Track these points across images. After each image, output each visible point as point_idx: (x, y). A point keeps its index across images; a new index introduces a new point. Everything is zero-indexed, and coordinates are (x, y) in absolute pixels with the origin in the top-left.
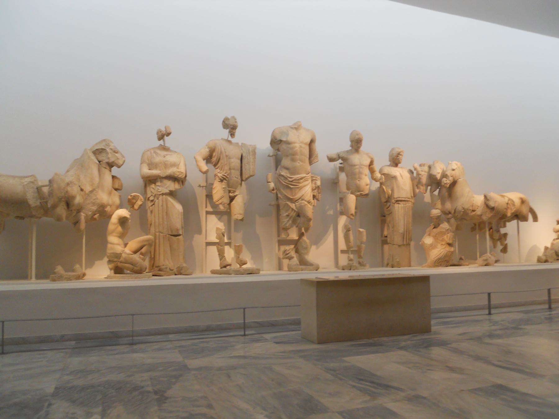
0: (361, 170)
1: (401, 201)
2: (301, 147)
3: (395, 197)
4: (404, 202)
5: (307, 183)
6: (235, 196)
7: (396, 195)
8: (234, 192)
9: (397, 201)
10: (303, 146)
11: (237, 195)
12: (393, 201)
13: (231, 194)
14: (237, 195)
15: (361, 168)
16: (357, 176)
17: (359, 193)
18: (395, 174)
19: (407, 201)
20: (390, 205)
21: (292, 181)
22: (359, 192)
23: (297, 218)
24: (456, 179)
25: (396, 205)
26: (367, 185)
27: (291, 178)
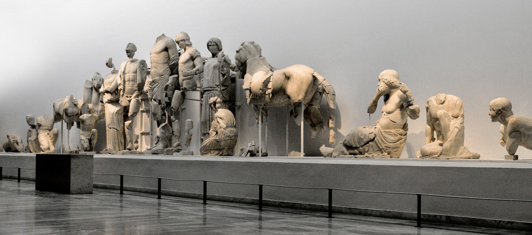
4: (207, 92)
8: (131, 97)
10: (155, 55)
19: (210, 90)
24: (242, 61)
26: (183, 80)
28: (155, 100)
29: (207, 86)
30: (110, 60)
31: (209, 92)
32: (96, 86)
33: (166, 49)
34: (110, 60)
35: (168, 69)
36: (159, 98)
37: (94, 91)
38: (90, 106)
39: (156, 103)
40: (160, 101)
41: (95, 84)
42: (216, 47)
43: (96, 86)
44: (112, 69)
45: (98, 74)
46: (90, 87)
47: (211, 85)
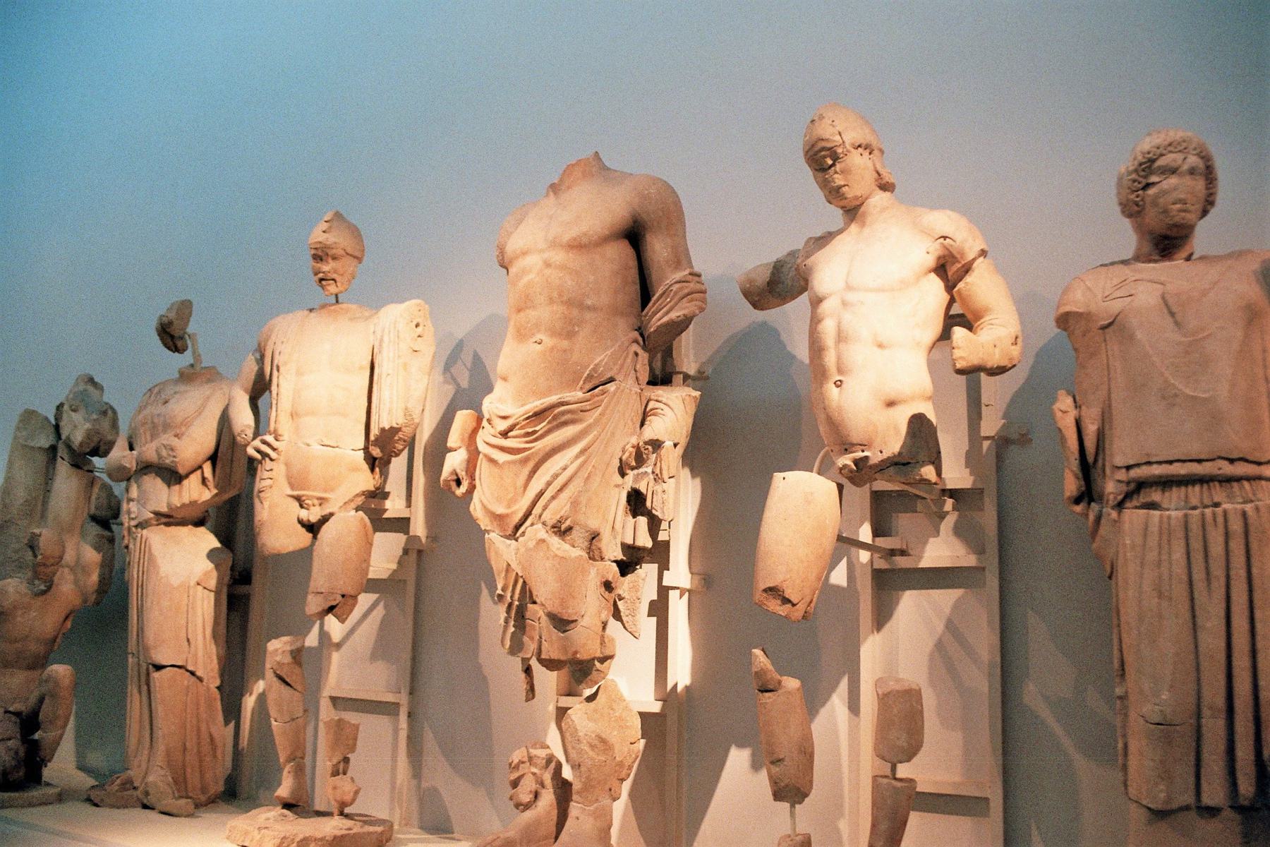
0: (847, 317)
1: (1166, 483)
2: (548, 265)
3: (1119, 460)
4: (1195, 492)
5: (569, 431)
6: (325, 519)
7: (1121, 451)
8: (322, 501)
9: (1141, 485)
10: (558, 257)
11: (331, 514)
12: (1111, 488)
13: (304, 514)
14: (331, 514)
15: (845, 304)
16: (830, 359)
17: (846, 460)
18: (1116, 306)
19: (1228, 480)
20: (1098, 519)
21: (505, 434)
22: (847, 448)
23: (530, 606)
25: (1133, 517)
27: (504, 418)
28: (561, 530)
29: (1195, 449)
30: (185, 308)
31: (1218, 494)
32: (78, 438)
33: (634, 235)
34: (185, 308)
35: (635, 347)
36: (594, 524)
37: (63, 467)
38: (46, 535)
39: (572, 551)
40: (594, 536)
41: (77, 429)
42: (1199, 185)
43: (78, 438)
44: (185, 359)
45: (91, 380)
46: (47, 446)
47: (1234, 438)
